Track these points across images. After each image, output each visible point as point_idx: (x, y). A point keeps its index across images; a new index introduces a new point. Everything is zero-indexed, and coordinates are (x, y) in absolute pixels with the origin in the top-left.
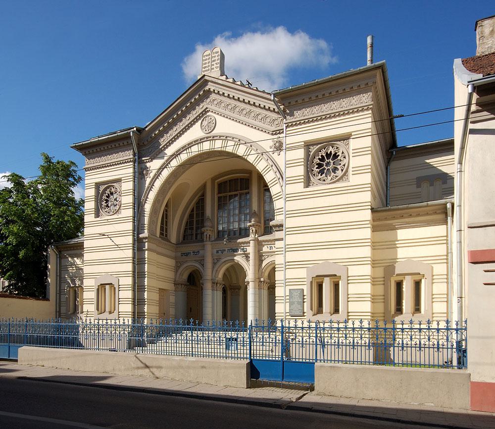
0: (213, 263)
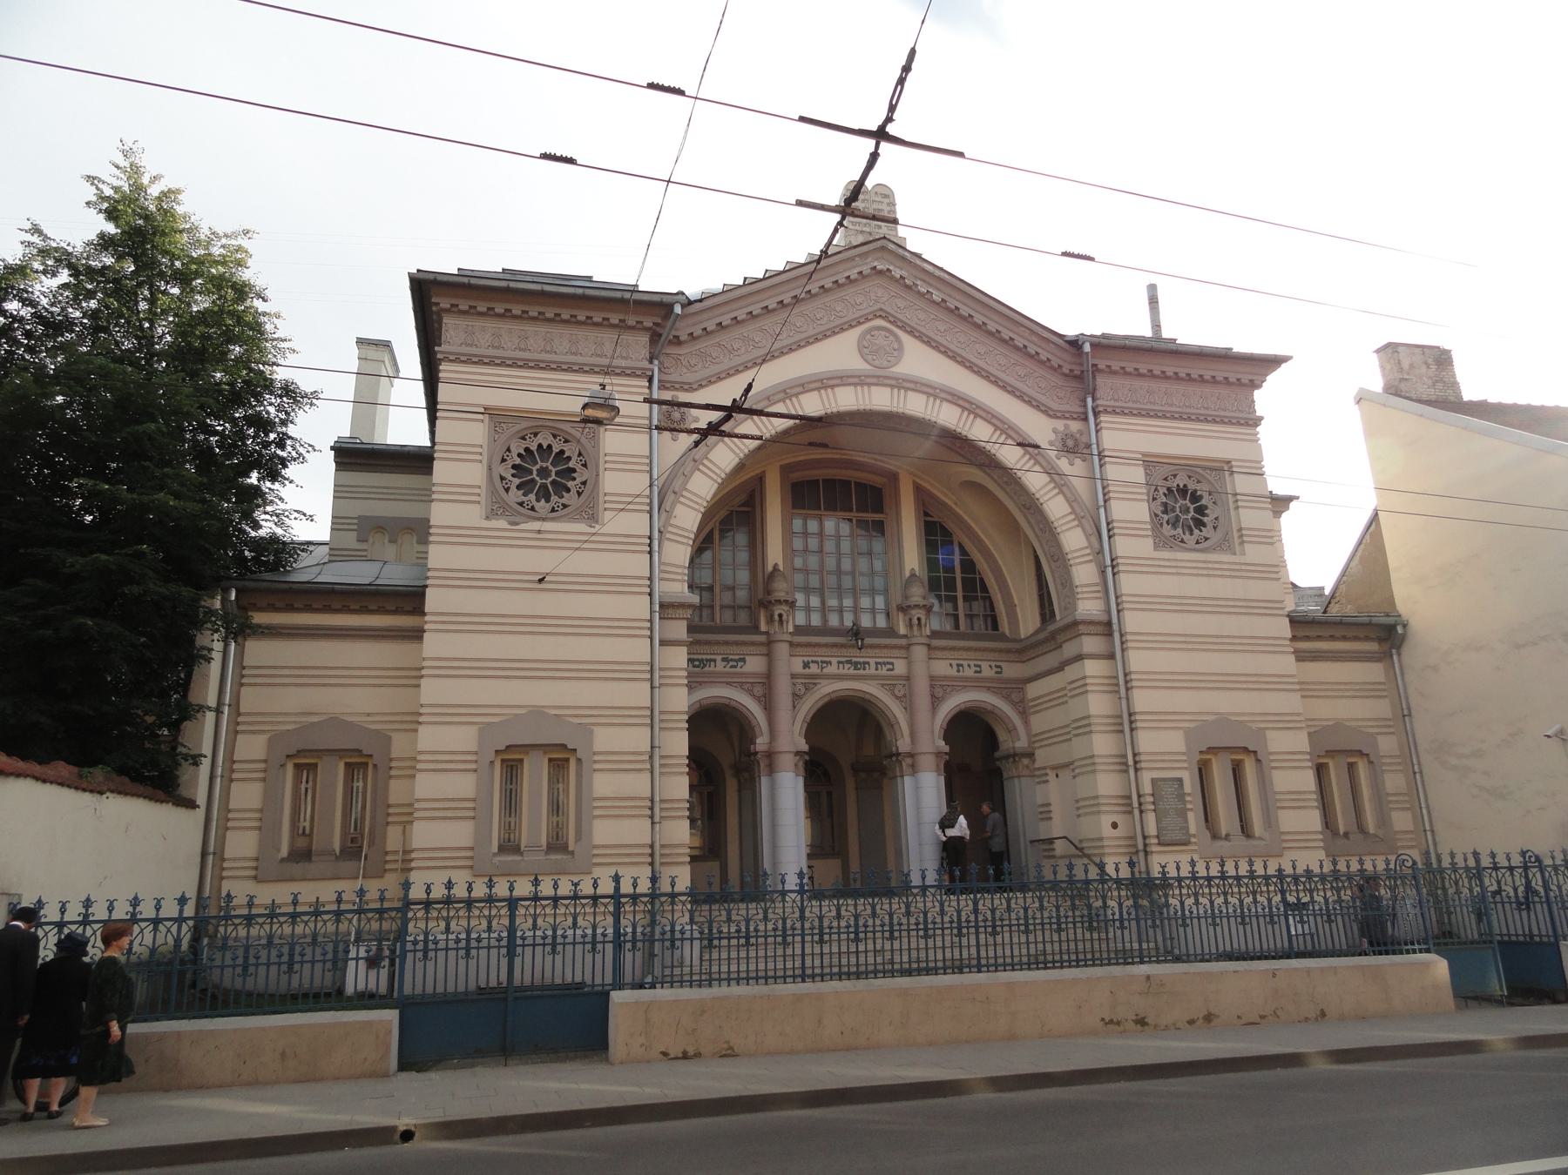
0: (794, 694)
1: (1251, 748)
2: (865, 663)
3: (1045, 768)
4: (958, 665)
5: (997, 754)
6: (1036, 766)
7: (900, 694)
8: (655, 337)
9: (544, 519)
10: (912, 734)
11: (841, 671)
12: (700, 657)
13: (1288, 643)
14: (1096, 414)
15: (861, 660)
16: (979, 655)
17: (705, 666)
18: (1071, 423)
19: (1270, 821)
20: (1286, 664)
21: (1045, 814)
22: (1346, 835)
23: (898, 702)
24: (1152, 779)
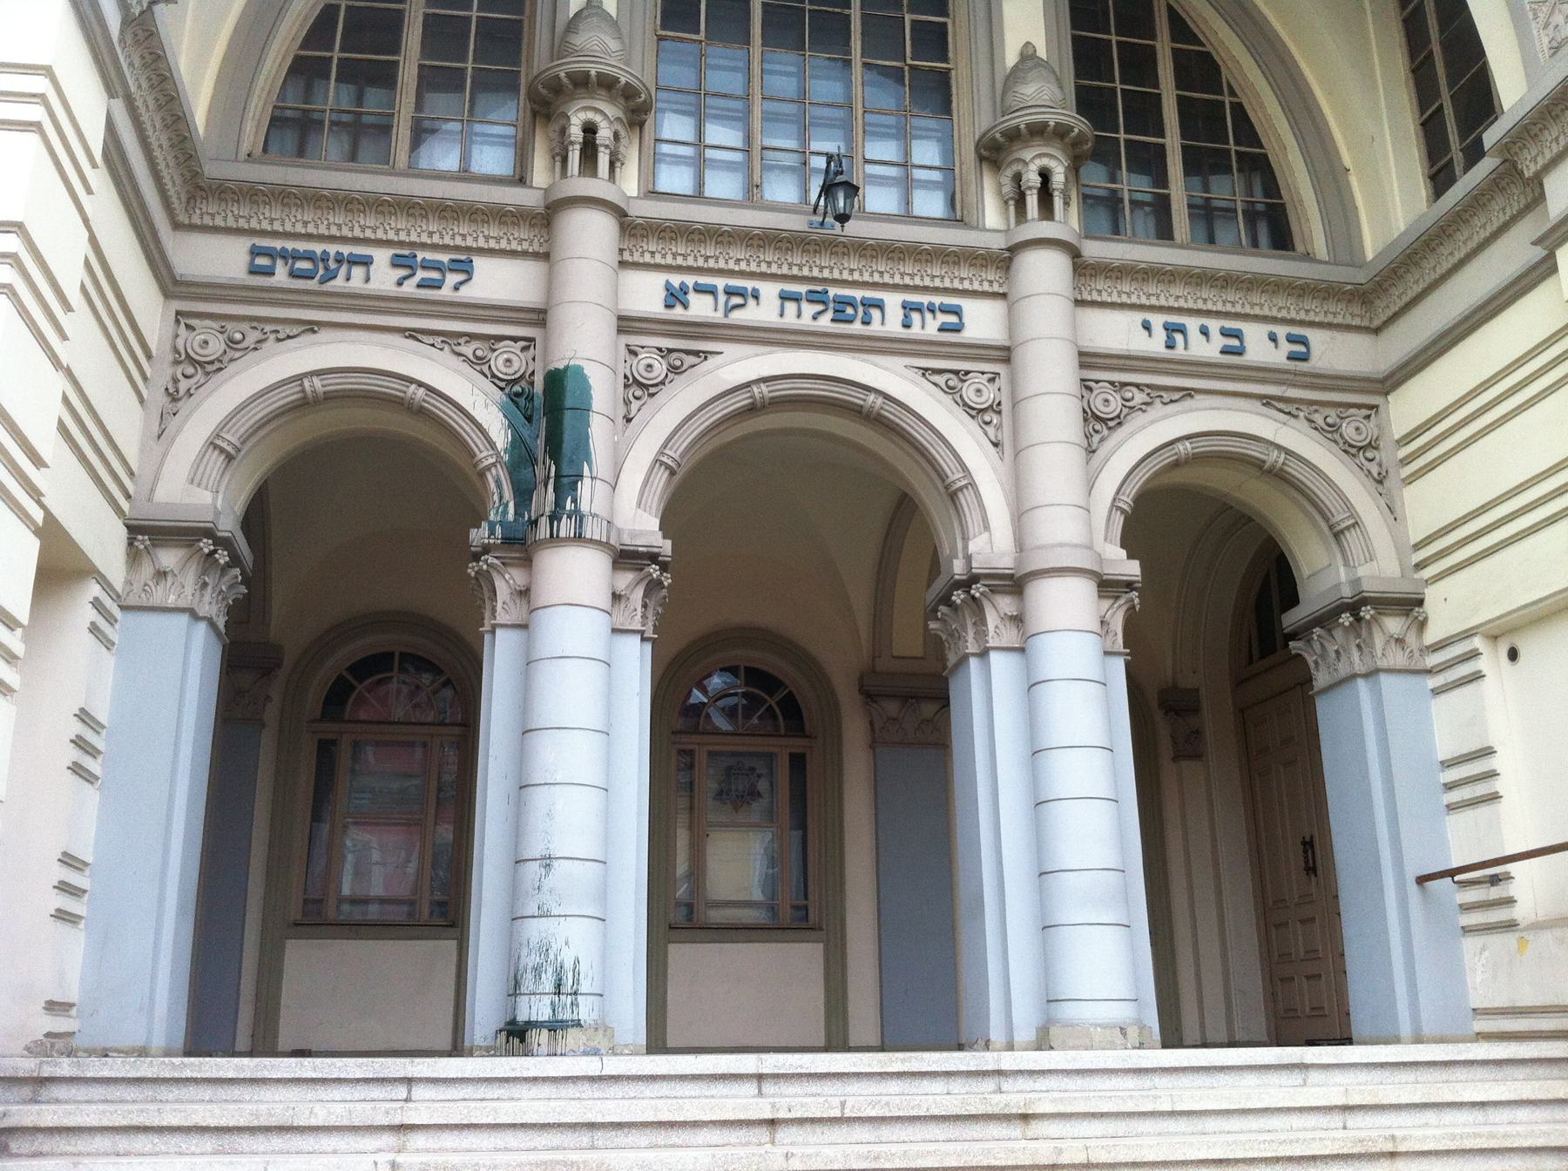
2: (869, 304)
3: (1467, 634)
4: (1171, 329)
5: (1292, 618)
6: (1432, 635)
10: (1020, 515)
11: (790, 319)
12: (318, 248)
15: (858, 294)
16: (1235, 300)
17: (330, 276)
23: (973, 425)
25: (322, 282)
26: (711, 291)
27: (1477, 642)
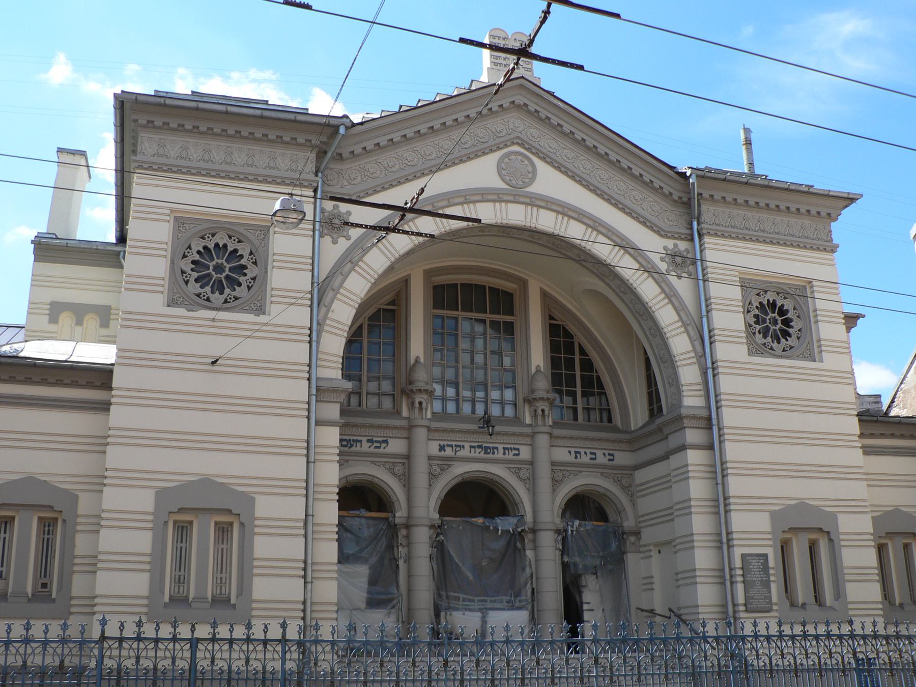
1: (825, 530)
2: (493, 448)
3: (650, 545)
4: (576, 452)
7: (524, 477)
8: (321, 154)
9: (218, 309)
11: (473, 454)
13: (857, 438)
14: (700, 236)
15: (491, 445)
16: (596, 444)
17: (352, 446)
18: (679, 242)
19: (839, 593)
20: (855, 457)
21: (648, 584)
22: (901, 605)
24: (742, 555)
25: (350, 448)
26: (451, 446)
27: (651, 548)
